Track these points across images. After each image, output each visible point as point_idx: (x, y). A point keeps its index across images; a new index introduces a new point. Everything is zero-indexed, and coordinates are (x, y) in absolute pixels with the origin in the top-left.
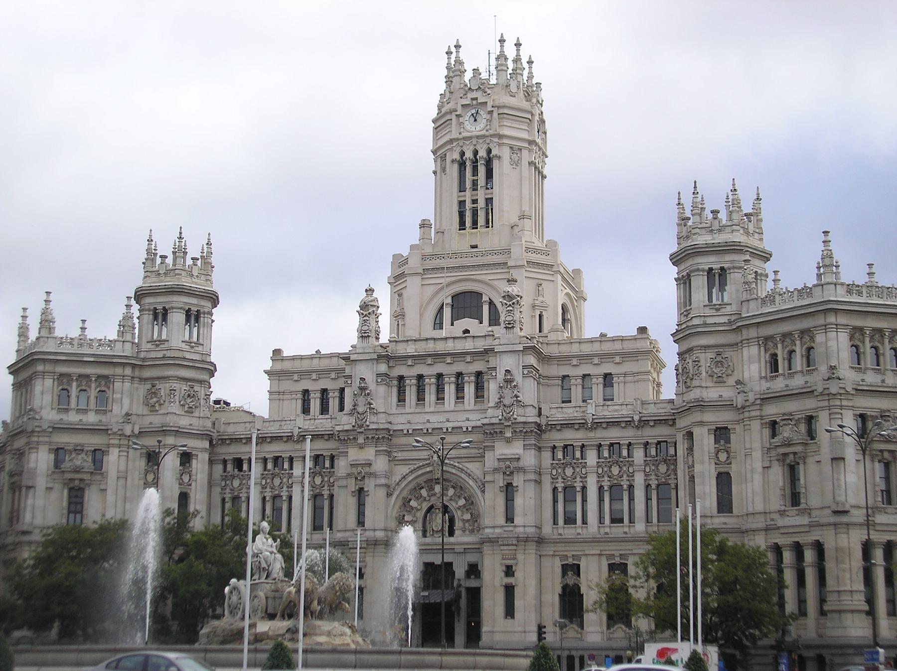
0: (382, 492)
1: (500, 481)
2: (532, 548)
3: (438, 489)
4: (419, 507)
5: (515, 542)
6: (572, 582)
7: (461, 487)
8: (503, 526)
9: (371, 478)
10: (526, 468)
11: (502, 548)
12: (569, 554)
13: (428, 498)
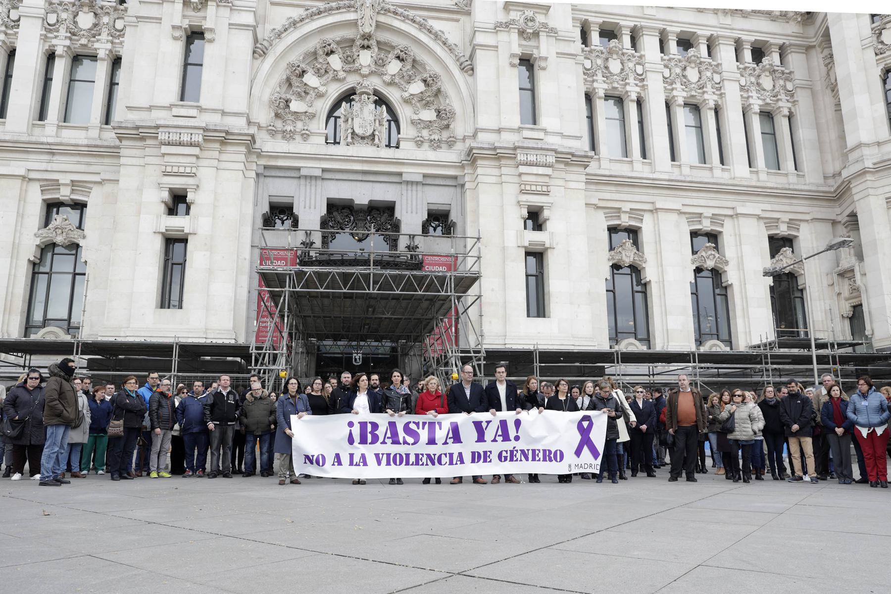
0: (243, 42)
1: (513, 44)
2: (576, 178)
3: (365, 58)
4: (322, 89)
5: (551, 159)
6: (632, 259)
7: (414, 61)
8: (520, 129)
9: (222, 10)
10: (559, 33)
11: (523, 169)
12: (626, 207)
13: (342, 74)
